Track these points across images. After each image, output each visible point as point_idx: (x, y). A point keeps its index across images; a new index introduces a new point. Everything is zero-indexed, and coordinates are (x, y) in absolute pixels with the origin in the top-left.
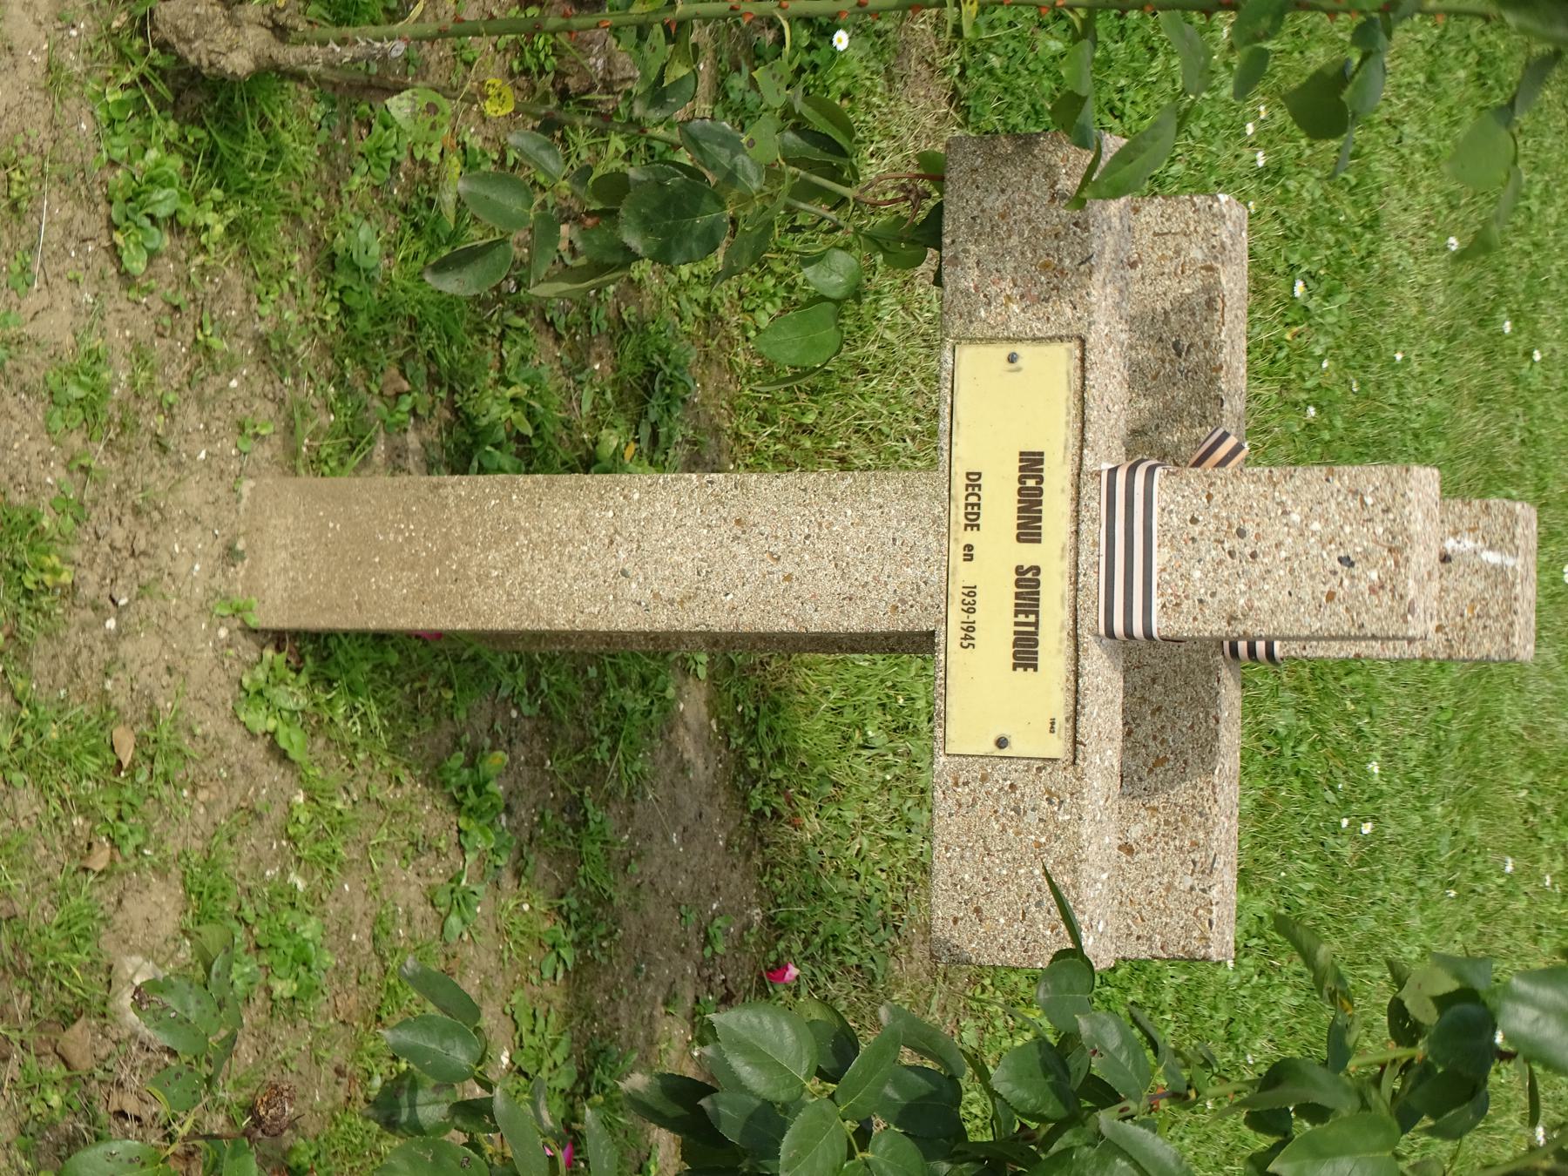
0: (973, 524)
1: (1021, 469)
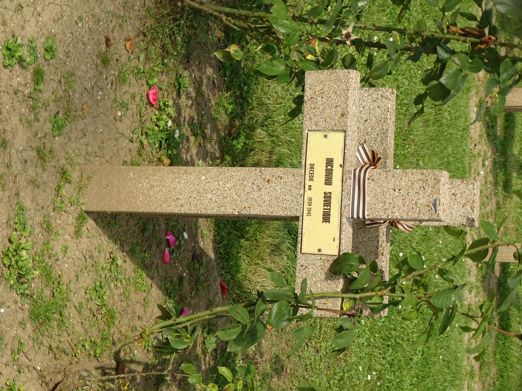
0: (311, 179)
1: (326, 163)
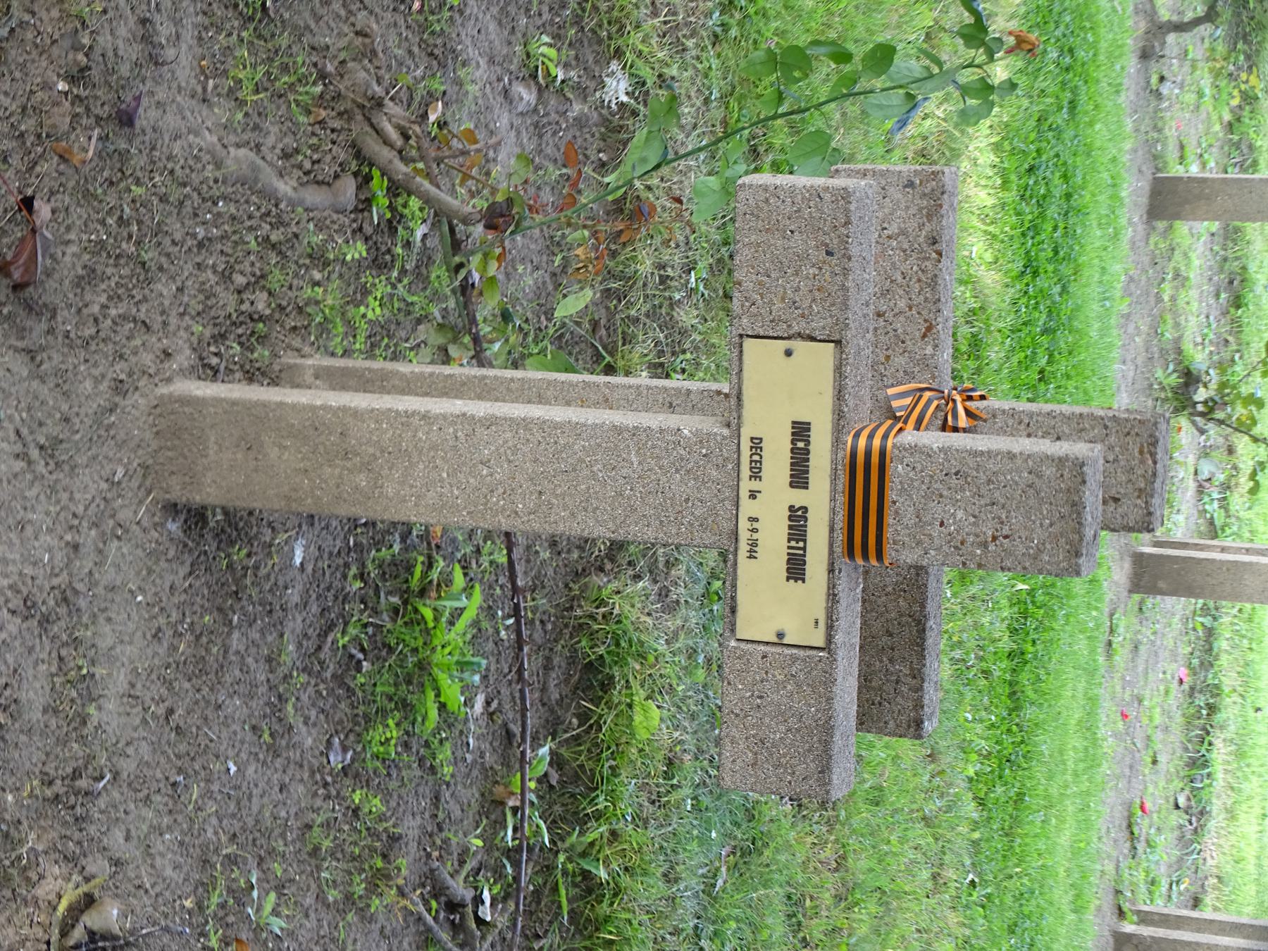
1: (793, 434)
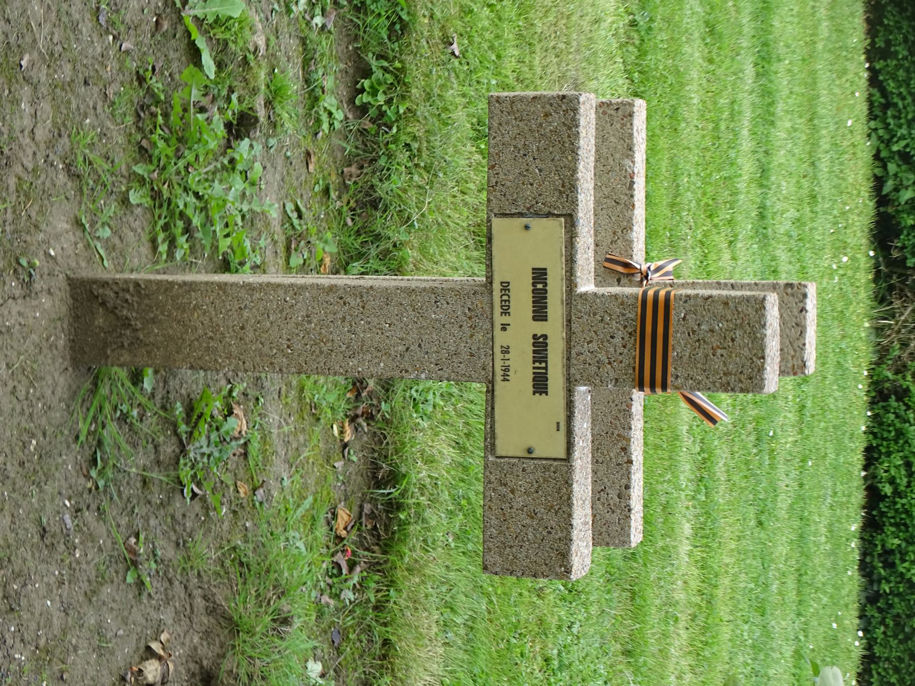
1: (533, 278)
